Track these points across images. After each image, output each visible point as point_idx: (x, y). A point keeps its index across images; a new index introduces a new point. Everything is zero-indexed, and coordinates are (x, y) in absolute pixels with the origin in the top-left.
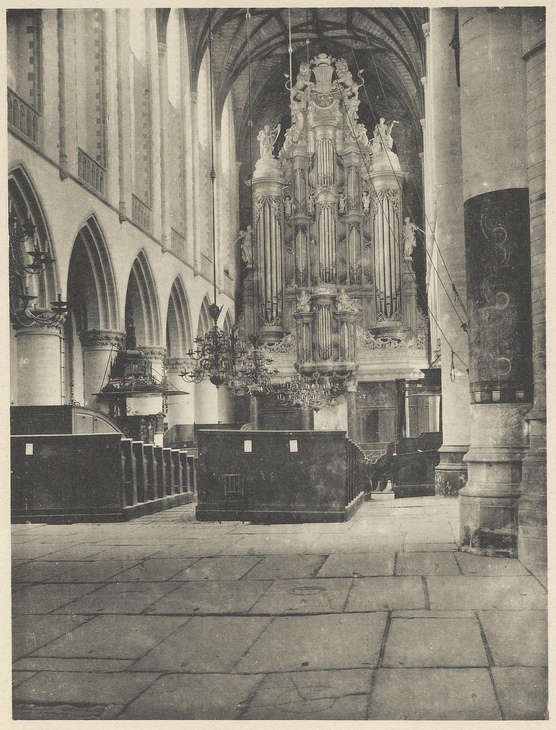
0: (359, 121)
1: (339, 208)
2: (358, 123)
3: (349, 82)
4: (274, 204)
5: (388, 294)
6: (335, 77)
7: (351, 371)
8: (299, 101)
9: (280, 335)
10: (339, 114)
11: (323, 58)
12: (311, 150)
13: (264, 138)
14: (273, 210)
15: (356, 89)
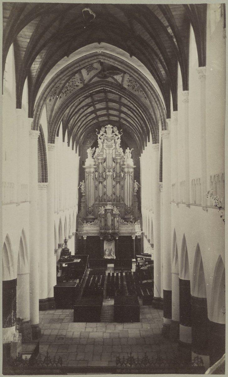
0: (120, 147)
1: (113, 176)
2: (120, 148)
3: (117, 134)
4: (92, 175)
5: (129, 206)
6: (113, 132)
7: (117, 233)
8: (101, 139)
9: (94, 219)
10: (114, 144)
11: (109, 126)
12: (104, 156)
13: (89, 151)
14: (92, 176)
15: (119, 136)
